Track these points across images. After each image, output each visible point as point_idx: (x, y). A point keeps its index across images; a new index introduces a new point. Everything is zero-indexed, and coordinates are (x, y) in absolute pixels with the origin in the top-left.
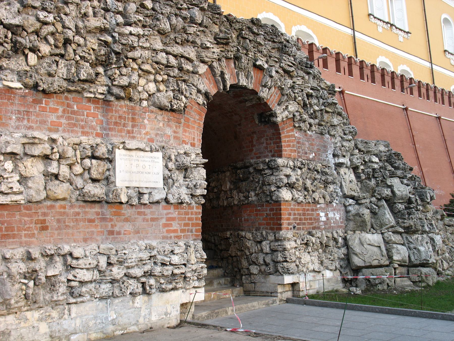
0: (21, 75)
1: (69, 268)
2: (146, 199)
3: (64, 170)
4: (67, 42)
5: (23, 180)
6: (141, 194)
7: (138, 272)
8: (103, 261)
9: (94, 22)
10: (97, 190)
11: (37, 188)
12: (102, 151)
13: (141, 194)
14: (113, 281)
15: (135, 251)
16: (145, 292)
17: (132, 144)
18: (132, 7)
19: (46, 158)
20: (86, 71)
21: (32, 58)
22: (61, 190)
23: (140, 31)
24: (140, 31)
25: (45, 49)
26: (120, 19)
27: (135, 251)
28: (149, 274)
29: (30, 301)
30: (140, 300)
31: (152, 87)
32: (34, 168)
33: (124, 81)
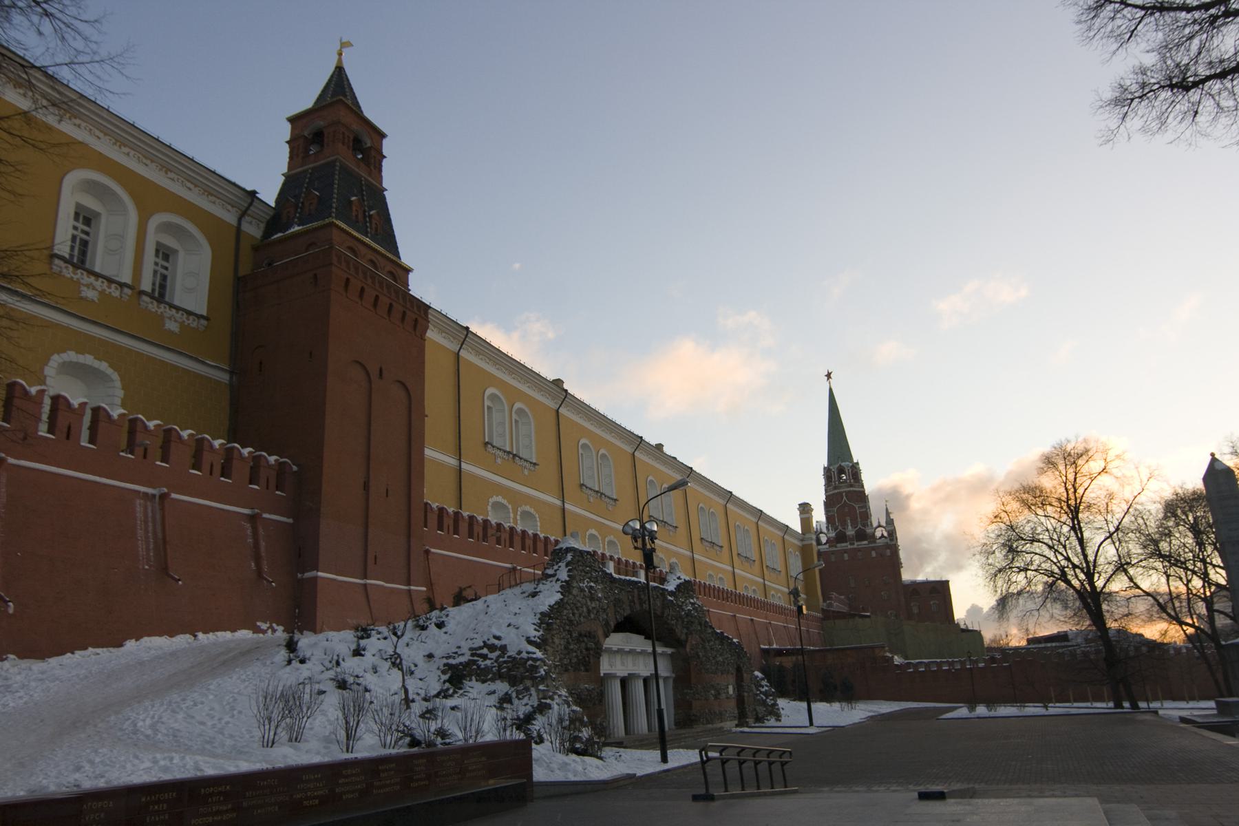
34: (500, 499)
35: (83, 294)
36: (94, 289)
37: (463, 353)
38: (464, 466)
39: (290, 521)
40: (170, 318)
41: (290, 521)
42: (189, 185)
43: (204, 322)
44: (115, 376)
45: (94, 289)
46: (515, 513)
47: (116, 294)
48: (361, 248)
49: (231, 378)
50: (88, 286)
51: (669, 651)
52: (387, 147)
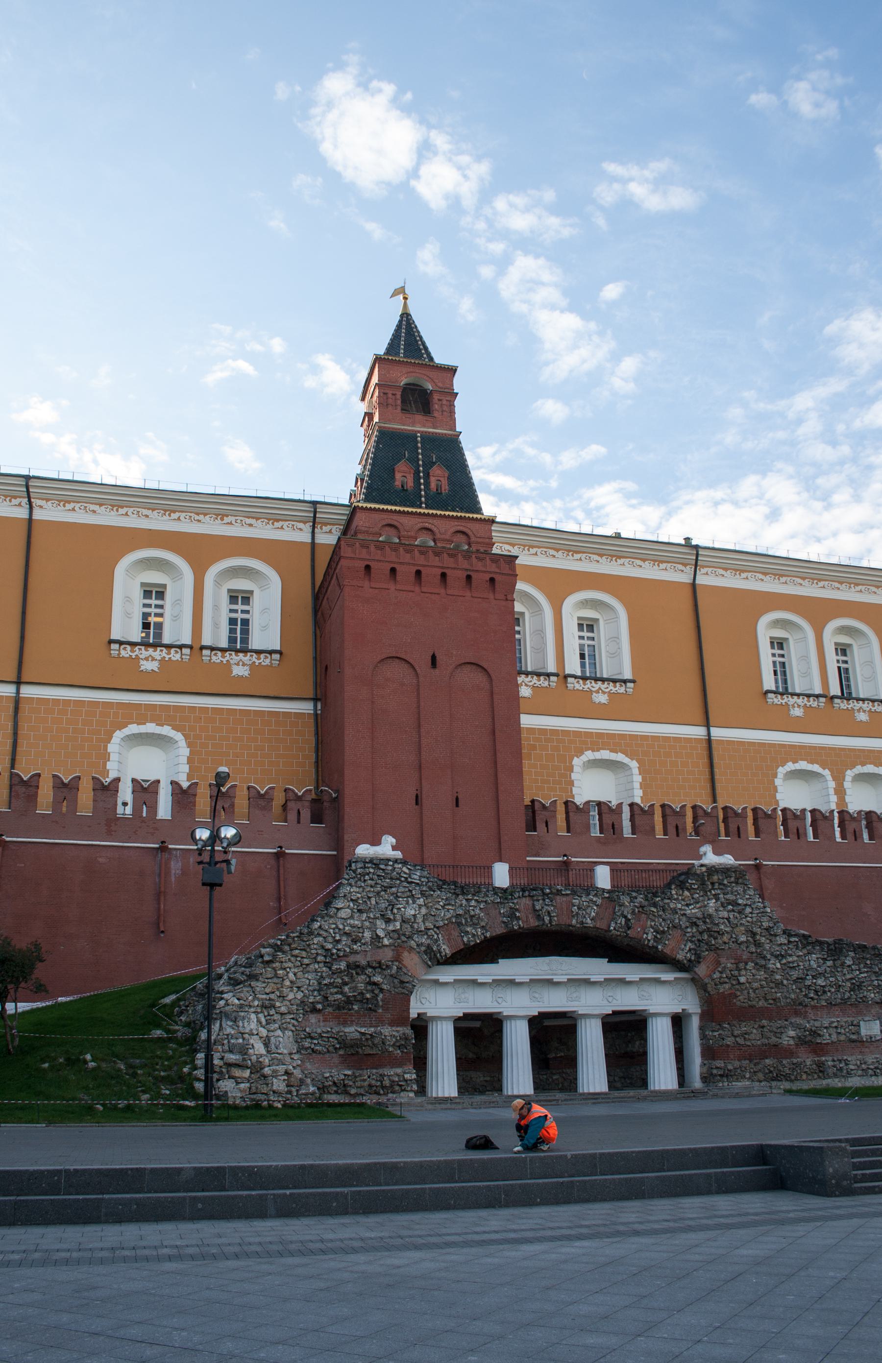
0: (826, 1000)
1: (846, 1064)
2: (873, 1039)
3: (843, 1031)
4: (840, 986)
5: (830, 1035)
6: (871, 1038)
7: (872, 1067)
8: (858, 1063)
9: (848, 976)
10: (854, 1037)
11: (834, 1037)
12: (855, 1022)
13: (871, 1038)
14: (863, 1070)
15: (870, 1059)
16: (875, 1075)
17: (867, 1018)
18: (862, 965)
19: (836, 1027)
20: (847, 995)
21: (829, 994)
22: (842, 1038)
23: (866, 975)
24: (866, 975)
25: (833, 990)
26: (858, 972)
27: (870, 1059)
28: (876, 1068)
29: (835, 1075)
30: (873, 1078)
31: (872, 995)
32: (831, 1031)
33: (861, 995)
34: (803, 765)
35: (142, 668)
36: (153, 659)
37: (701, 580)
38: (716, 732)
39: (335, 853)
40: (238, 664)
41: (335, 853)
42: (249, 521)
43: (277, 656)
44: (178, 736)
45: (153, 659)
46: (839, 779)
47: (178, 657)
48: (404, 520)
49: (315, 706)
50: (147, 659)
51: (669, 976)
52: (459, 383)
